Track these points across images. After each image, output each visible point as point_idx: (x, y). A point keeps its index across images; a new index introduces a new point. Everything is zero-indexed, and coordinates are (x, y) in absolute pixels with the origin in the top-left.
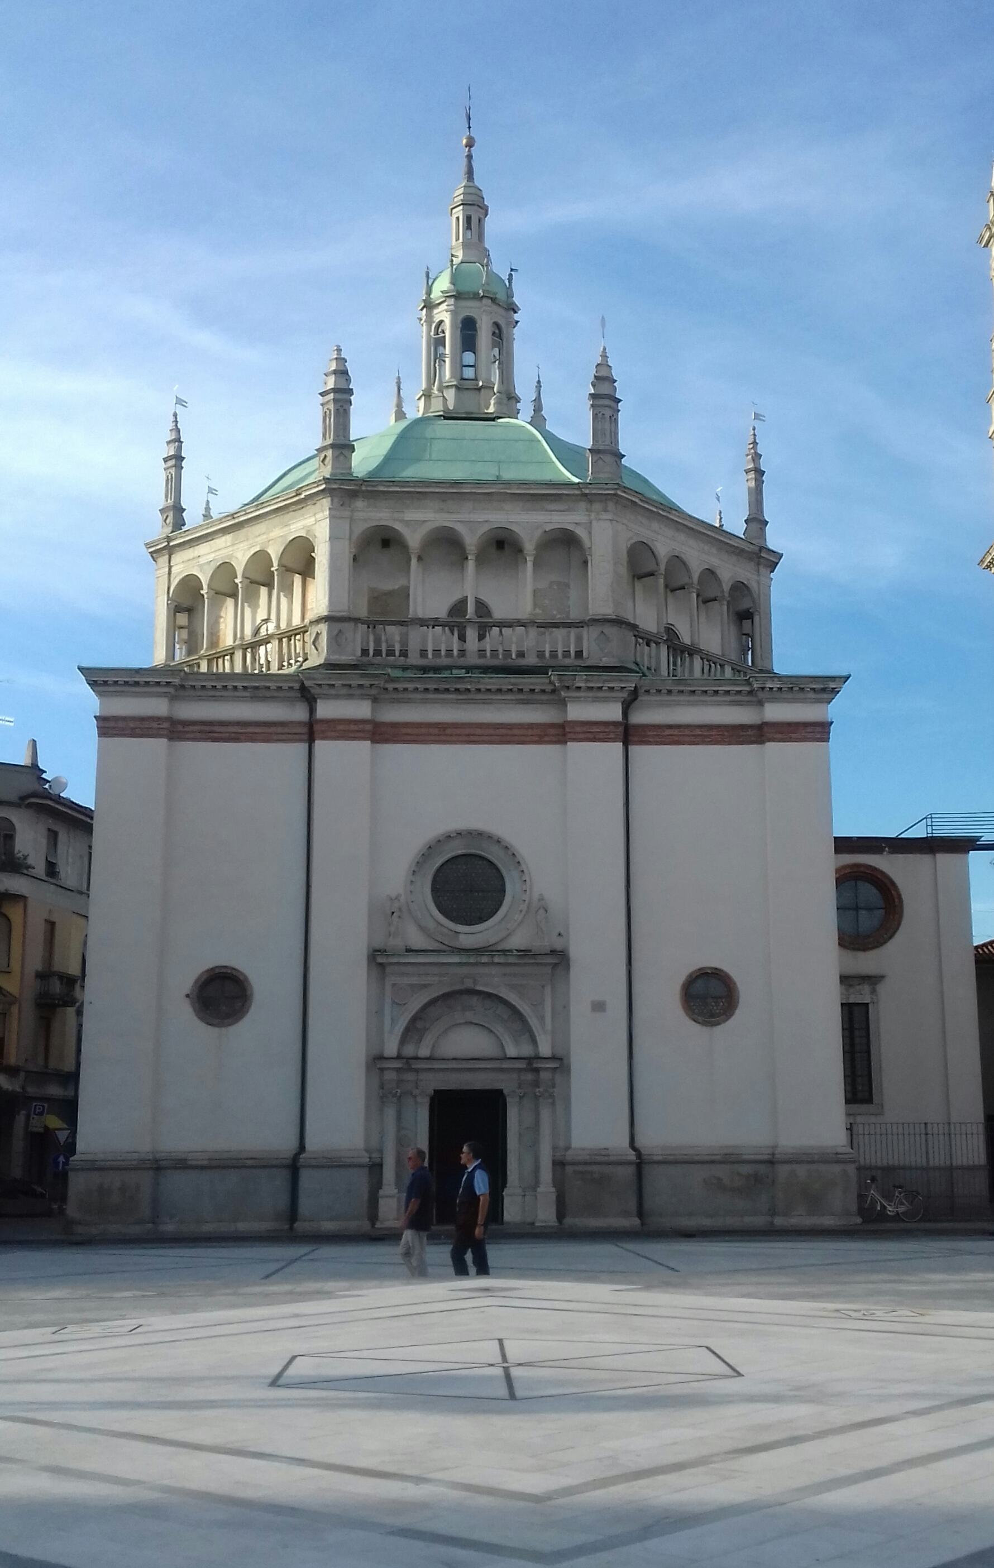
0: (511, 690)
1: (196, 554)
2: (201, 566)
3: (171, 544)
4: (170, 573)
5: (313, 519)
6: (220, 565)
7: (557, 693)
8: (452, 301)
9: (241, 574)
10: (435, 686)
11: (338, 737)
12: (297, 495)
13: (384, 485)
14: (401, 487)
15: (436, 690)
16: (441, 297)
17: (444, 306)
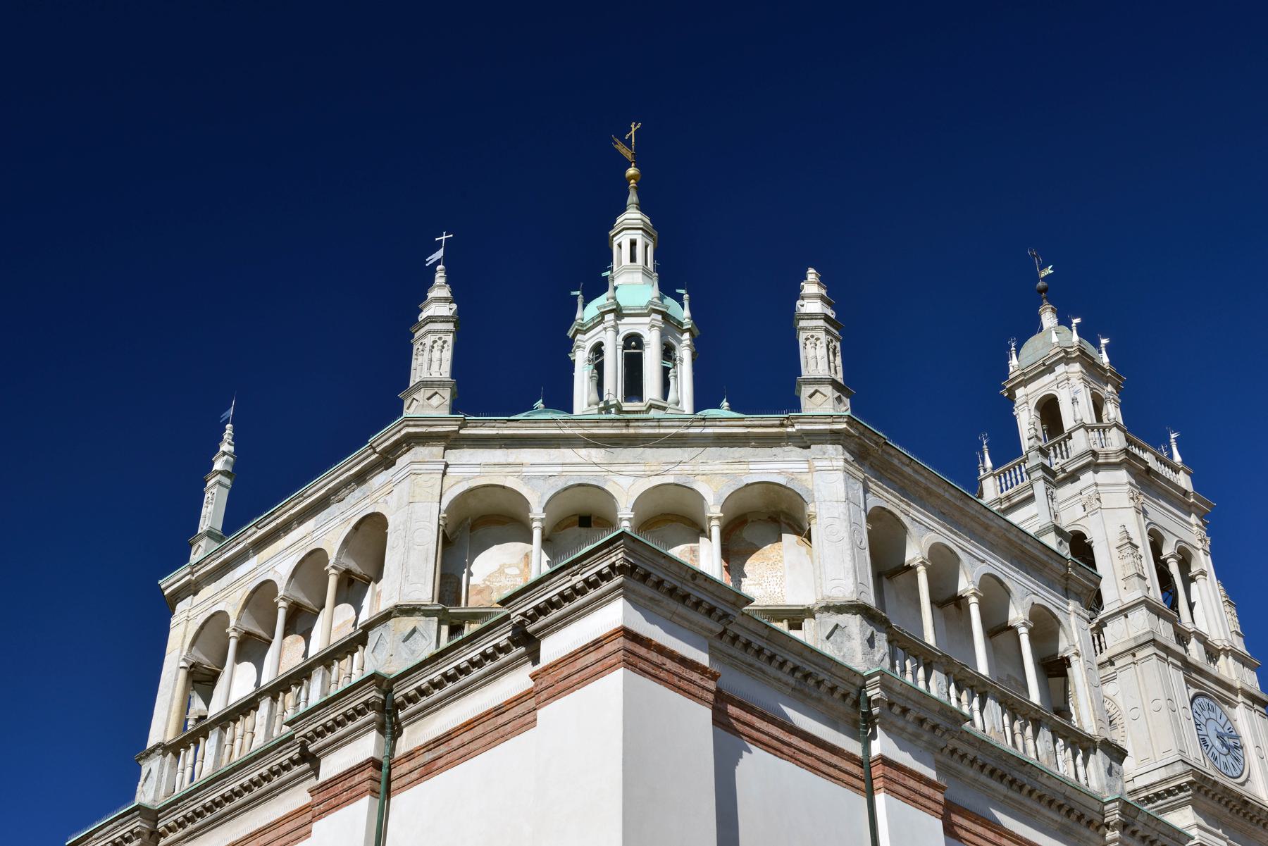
0: (1060, 807)
1: (511, 460)
2: (527, 479)
3: (462, 432)
4: (444, 474)
5: (806, 466)
6: (572, 486)
7: (1101, 831)
8: (660, 317)
9: (630, 505)
10: (994, 765)
11: (908, 798)
12: (782, 425)
13: (899, 459)
14: (916, 471)
15: (992, 772)
16: (642, 308)
17: (647, 320)
